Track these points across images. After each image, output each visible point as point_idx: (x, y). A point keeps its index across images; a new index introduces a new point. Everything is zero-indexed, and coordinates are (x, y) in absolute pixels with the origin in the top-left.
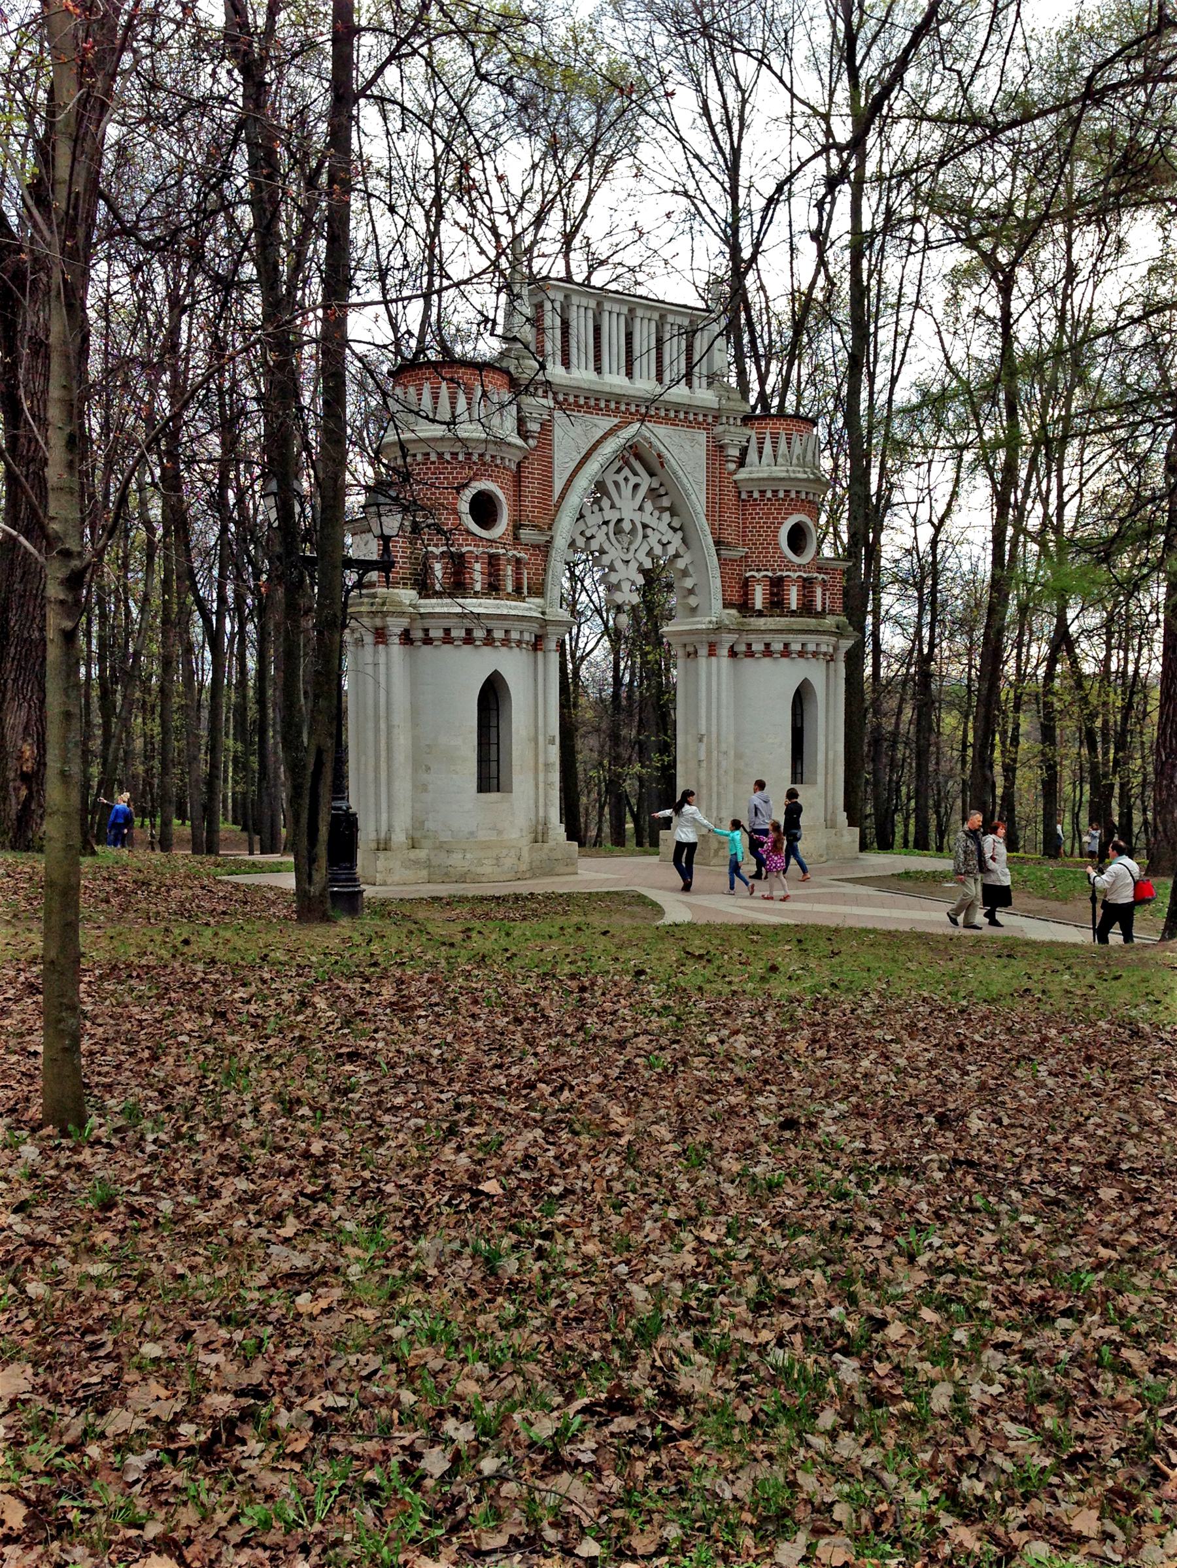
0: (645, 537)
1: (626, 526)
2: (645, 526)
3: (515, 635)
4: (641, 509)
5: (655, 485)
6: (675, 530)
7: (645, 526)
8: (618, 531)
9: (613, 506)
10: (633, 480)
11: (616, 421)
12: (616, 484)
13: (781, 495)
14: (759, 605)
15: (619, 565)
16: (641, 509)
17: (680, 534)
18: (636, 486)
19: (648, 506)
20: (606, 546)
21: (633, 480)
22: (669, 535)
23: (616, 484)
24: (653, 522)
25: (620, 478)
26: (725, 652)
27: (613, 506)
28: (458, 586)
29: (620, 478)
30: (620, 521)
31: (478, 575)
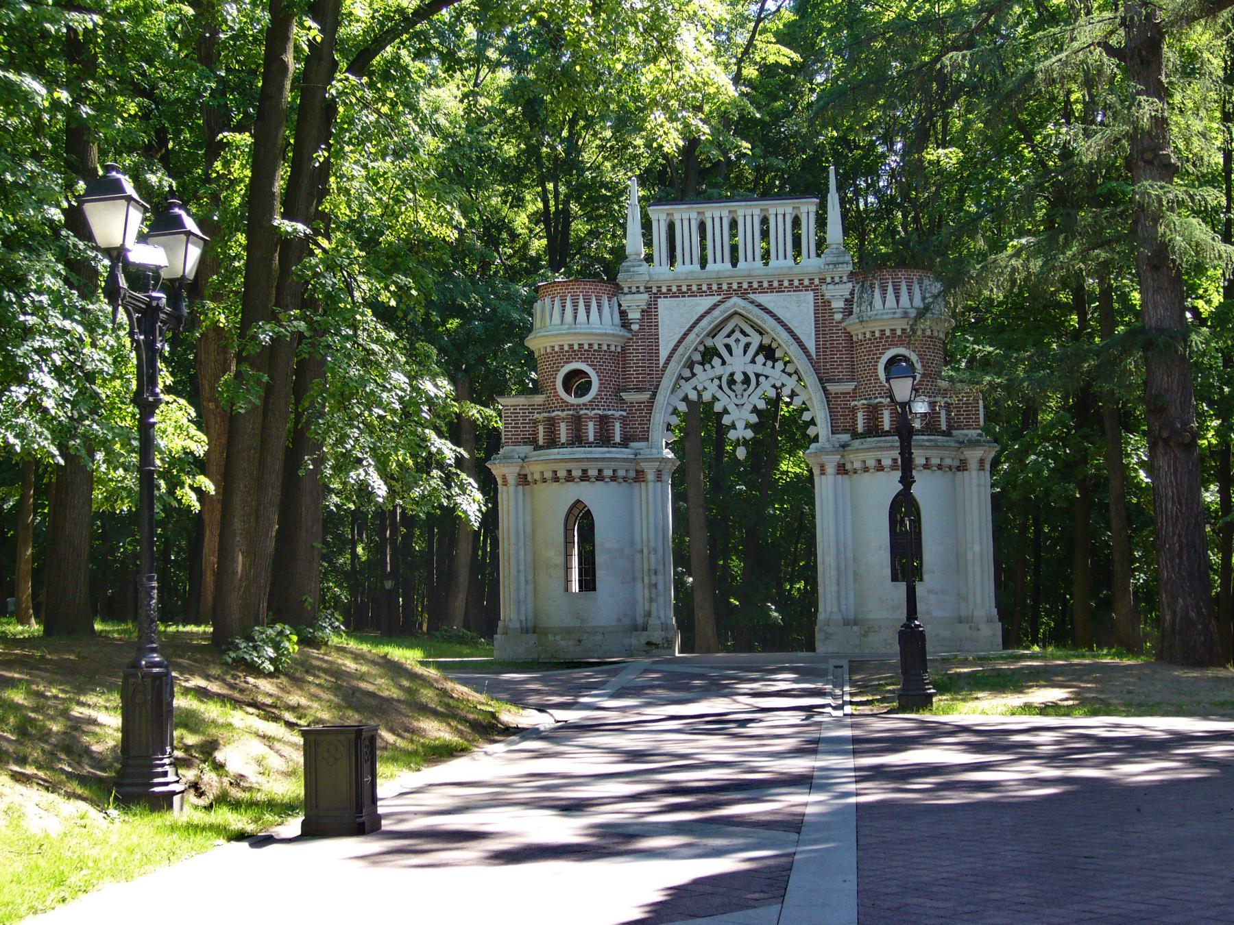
0: (758, 384)
1: (739, 377)
2: (757, 376)
3: (621, 473)
4: (753, 361)
5: (766, 341)
6: (790, 375)
7: (757, 376)
8: (731, 382)
9: (724, 363)
10: (744, 340)
11: (719, 298)
12: (728, 347)
13: (877, 334)
14: (860, 429)
15: (731, 408)
16: (753, 361)
17: (795, 377)
18: (747, 346)
19: (760, 359)
20: (719, 394)
21: (744, 340)
22: (785, 378)
23: (728, 347)
24: (767, 370)
25: (731, 341)
26: (830, 470)
27: (724, 363)
28: (552, 442)
29: (731, 341)
30: (732, 374)
31: (563, 433)
